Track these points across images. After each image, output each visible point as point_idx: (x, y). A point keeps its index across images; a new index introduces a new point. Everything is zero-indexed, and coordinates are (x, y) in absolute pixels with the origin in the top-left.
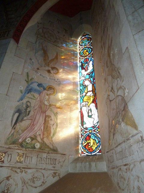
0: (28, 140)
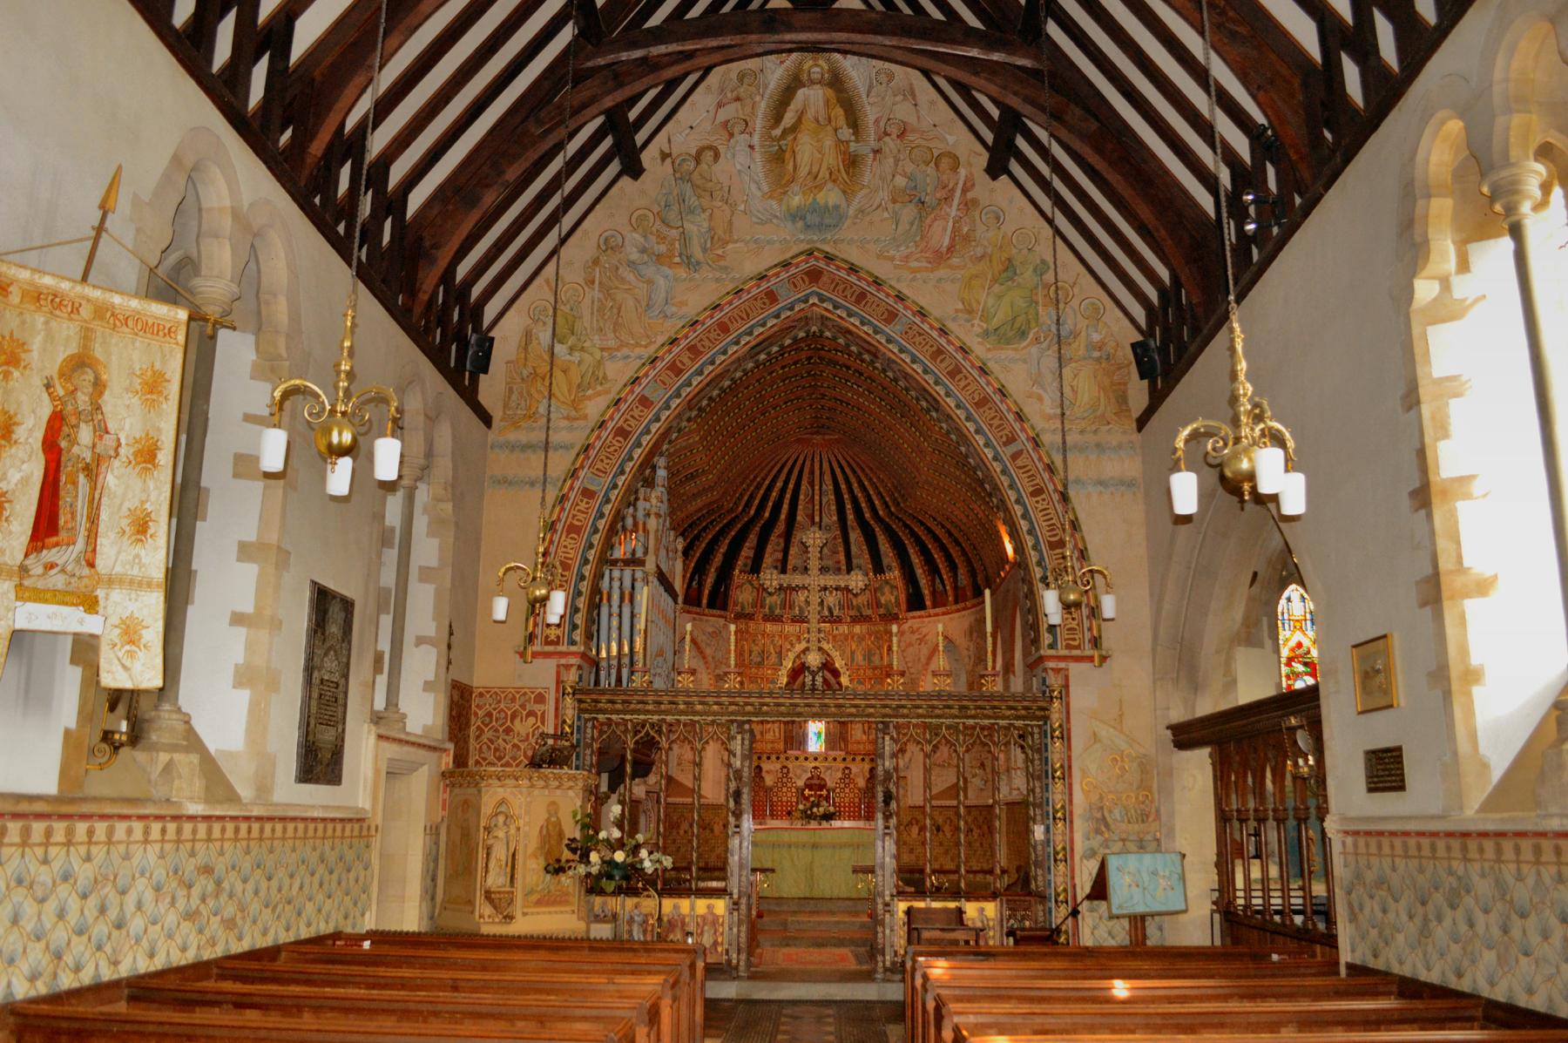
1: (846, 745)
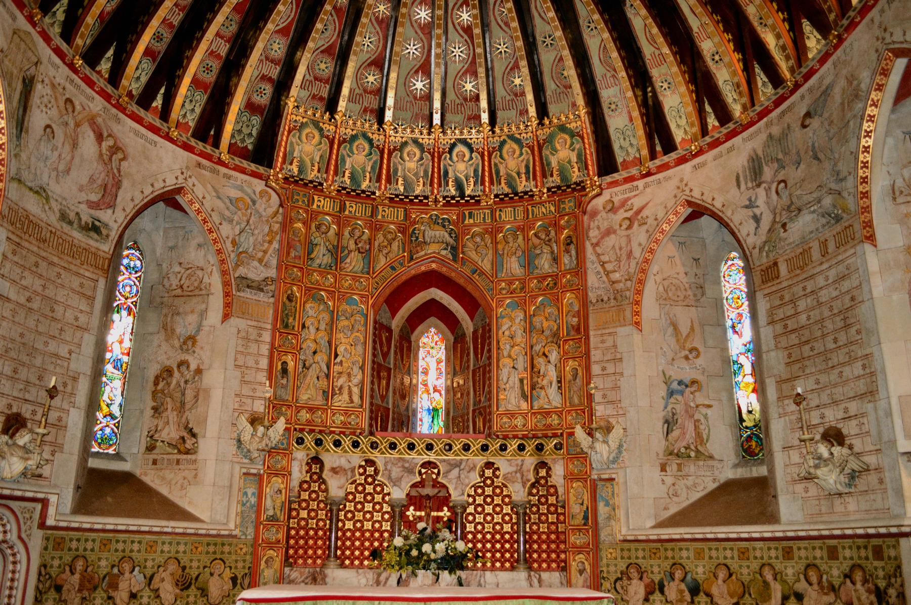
0: (683, 450)
1: (487, 421)
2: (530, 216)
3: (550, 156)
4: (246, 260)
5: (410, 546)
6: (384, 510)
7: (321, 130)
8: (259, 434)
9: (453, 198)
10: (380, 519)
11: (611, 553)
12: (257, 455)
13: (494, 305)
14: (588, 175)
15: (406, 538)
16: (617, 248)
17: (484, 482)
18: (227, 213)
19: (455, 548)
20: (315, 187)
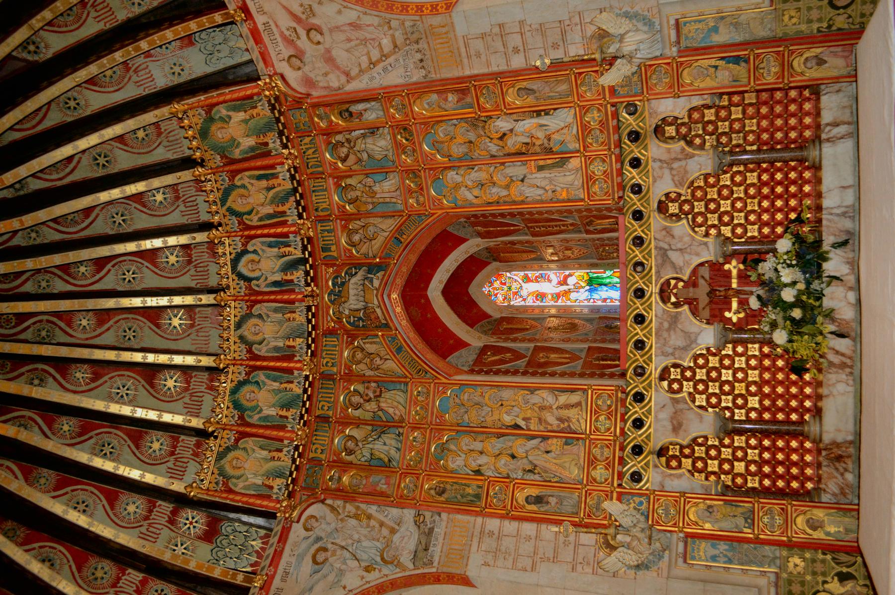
2: (320, 169)
3: (242, 148)
4: (392, 552)
5: (785, 319)
6: (730, 353)
7: (228, 450)
8: (628, 539)
9: (307, 273)
10: (743, 359)
11: (791, 17)
12: (658, 545)
13: (440, 212)
14: (259, 94)
15: (774, 325)
16: (349, 45)
17: (687, 214)
18: (331, 578)
19: (787, 253)
20: (300, 456)
